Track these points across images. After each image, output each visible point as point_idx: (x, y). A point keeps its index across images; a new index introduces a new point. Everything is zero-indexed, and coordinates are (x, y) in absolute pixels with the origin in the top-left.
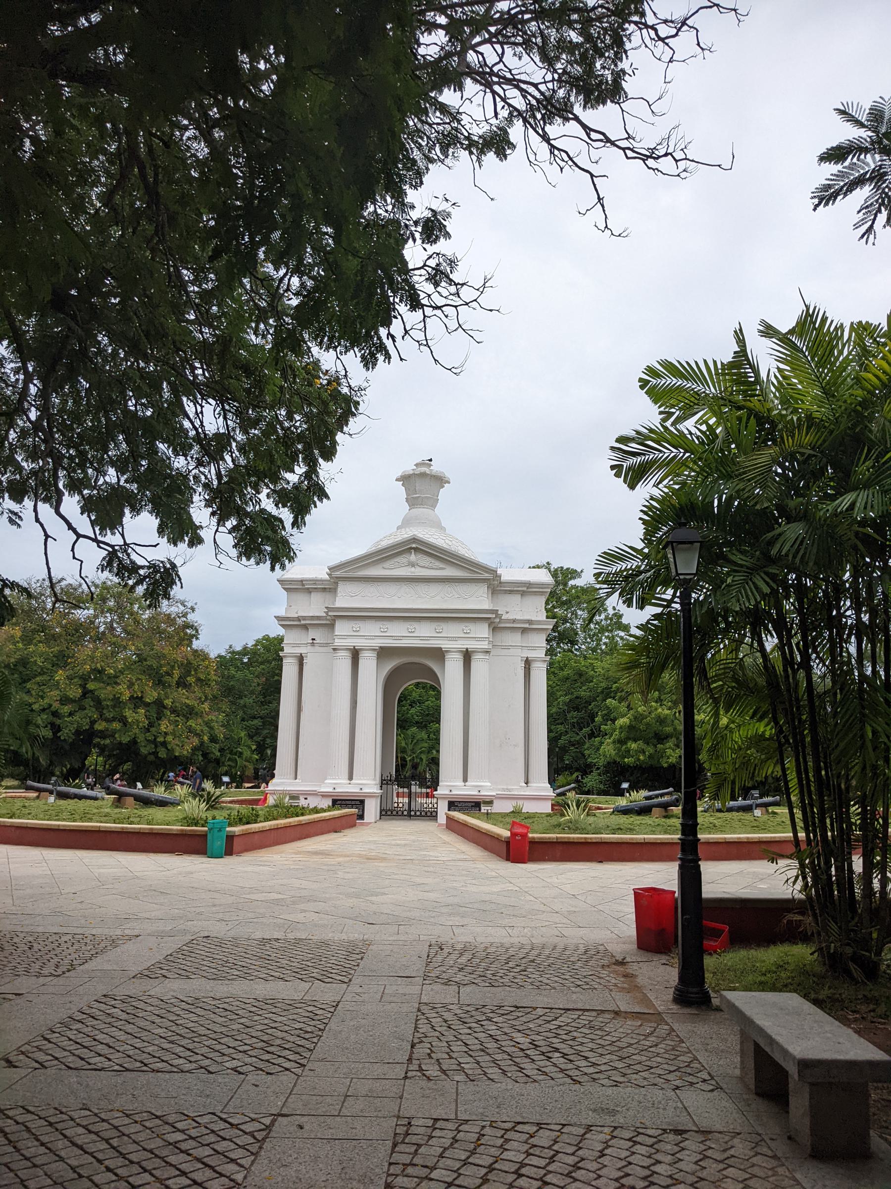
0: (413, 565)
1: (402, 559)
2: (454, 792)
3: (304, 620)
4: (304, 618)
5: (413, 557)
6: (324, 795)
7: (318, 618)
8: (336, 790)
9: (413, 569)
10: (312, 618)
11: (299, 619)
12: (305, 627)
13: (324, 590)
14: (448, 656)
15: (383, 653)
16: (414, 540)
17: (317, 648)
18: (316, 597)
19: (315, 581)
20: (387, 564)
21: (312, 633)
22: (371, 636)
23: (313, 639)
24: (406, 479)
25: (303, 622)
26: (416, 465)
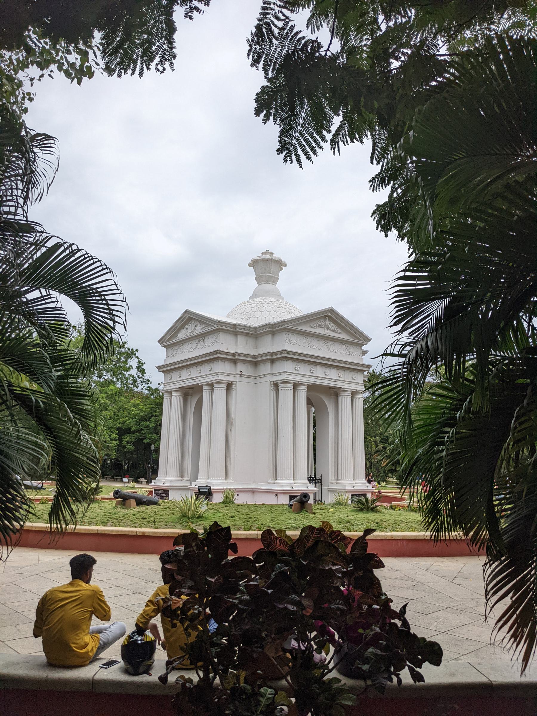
0: (328, 328)
1: (321, 323)
2: (356, 488)
4: (239, 354)
5: (328, 322)
6: (284, 493)
7: (248, 356)
8: (295, 489)
9: (326, 331)
11: (234, 355)
12: (235, 362)
13: (247, 335)
14: (342, 394)
15: (311, 388)
16: (331, 310)
17: (243, 379)
18: (241, 339)
19: (245, 327)
21: (240, 367)
22: (307, 375)
23: (241, 371)
24: (254, 263)
25: (237, 357)
26: (263, 253)
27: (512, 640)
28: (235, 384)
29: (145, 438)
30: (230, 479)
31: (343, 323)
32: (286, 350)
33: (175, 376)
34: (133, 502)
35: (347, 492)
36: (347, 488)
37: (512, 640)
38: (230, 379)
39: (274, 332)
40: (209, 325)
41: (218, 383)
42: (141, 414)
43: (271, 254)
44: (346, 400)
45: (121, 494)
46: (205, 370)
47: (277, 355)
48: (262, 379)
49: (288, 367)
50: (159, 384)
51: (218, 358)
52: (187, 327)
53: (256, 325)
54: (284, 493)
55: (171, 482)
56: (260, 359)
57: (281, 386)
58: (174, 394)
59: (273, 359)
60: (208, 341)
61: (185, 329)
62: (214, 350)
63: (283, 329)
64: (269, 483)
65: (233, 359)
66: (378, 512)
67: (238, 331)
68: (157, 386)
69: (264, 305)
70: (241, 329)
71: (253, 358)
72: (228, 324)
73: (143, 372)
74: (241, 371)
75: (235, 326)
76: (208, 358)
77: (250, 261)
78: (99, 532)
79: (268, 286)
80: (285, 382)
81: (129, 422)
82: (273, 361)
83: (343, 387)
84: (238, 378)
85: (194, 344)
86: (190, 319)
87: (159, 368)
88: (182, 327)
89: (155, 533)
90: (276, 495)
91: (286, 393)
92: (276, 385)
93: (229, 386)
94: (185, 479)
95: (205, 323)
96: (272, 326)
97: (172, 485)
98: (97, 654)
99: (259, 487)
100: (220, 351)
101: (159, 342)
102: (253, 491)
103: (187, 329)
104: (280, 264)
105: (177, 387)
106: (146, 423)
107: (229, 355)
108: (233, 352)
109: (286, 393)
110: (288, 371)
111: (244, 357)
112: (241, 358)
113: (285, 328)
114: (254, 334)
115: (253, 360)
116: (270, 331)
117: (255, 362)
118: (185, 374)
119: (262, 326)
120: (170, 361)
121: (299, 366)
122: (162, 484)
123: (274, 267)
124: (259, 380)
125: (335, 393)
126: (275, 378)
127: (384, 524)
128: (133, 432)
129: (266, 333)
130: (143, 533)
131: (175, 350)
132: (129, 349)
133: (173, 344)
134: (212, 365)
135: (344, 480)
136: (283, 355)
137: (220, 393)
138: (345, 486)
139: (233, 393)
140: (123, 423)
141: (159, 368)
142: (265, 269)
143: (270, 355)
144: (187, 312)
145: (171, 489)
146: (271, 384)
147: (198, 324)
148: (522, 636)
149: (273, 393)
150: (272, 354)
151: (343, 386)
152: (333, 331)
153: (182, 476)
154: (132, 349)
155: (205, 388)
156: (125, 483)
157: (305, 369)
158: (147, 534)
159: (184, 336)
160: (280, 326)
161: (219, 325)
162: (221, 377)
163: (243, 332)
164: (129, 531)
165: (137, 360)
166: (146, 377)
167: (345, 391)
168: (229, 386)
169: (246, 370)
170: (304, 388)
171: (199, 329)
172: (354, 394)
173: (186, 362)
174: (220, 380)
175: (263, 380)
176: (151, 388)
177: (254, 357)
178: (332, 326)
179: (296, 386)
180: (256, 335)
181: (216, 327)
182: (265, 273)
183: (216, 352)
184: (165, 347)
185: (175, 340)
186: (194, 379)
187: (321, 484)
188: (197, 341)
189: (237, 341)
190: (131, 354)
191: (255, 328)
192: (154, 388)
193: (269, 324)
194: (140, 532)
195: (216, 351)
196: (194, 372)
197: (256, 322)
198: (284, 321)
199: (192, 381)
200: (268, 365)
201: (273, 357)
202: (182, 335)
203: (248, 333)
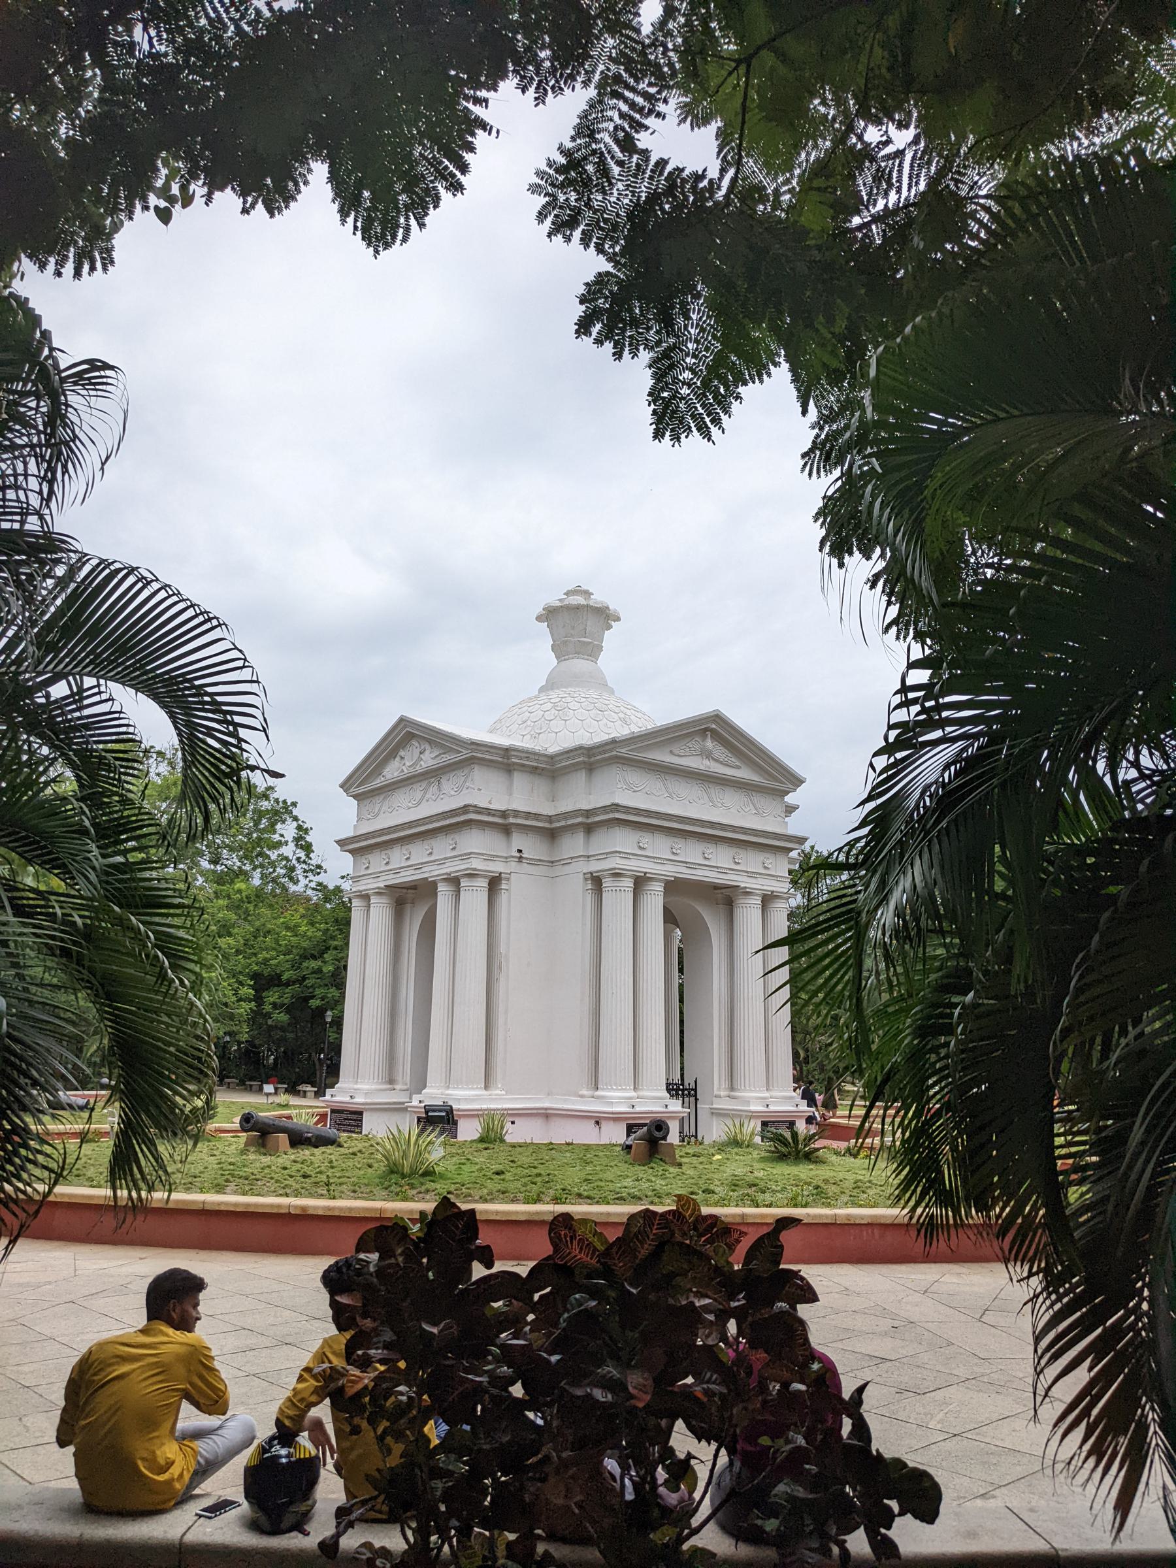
0: (709, 756)
1: (695, 744)
2: (772, 1108)
3: (515, 817)
4: (516, 814)
5: (709, 744)
6: (616, 1118)
7: (536, 816)
8: (637, 1109)
9: (706, 762)
10: (528, 815)
11: (504, 814)
13: (534, 771)
14: (741, 901)
15: (673, 887)
16: (717, 718)
17: (525, 867)
18: (520, 781)
19: (529, 754)
20: (676, 748)
21: (519, 841)
22: (665, 858)
23: (520, 851)
24: (550, 615)
25: (512, 820)
27: (1092, 1461)
28: (508, 879)
29: (312, 997)
30: (497, 1088)
31: (745, 746)
32: (617, 805)
33: (377, 862)
34: (283, 1138)
35: (752, 1116)
36: (753, 1108)
37: (1092, 1461)
38: (497, 867)
39: (591, 764)
40: (450, 750)
41: (471, 876)
42: (305, 944)
43: (587, 594)
44: (749, 915)
45: (257, 1123)
46: (441, 847)
47: (597, 815)
48: (566, 867)
49: (623, 840)
50: (343, 877)
51: (470, 821)
52: (402, 753)
53: (553, 749)
54: (615, 1120)
55: (368, 1093)
56: (563, 823)
57: (607, 883)
58: (373, 900)
59: (590, 823)
60: (449, 784)
61: (398, 759)
62: (462, 804)
63: (611, 758)
64: (582, 1096)
65: (504, 824)
66: (819, 1161)
67: (514, 764)
68: (339, 882)
69: (572, 705)
70: (521, 758)
71: (545, 821)
72: (492, 747)
73: (308, 848)
74: (520, 851)
75: (507, 751)
76: (448, 822)
77: (539, 610)
78: (208, 1207)
79: (579, 665)
80: (617, 875)
81: (280, 962)
82: (589, 829)
83: (742, 885)
84: (513, 866)
85: (417, 791)
86: (410, 736)
87: (341, 843)
88: (393, 754)
89: (329, 1208)
90: (597, 1123)
91: (618, 898)
92: (596, 882)
93: (494, 883)
94: (398, 1087)
95: (442, 746)
96: (589, 751)
97: (369, 1101)
98: (192, 1485)
99: (560, 1106)
100: (475, 806)
101: (342, 786)
102: (546, 1115)
103: (402, 758)
104: (605, 616)
105: (382, 885)
106: (314, 964)
107: (494, 815)
108: (503, 808)
109: (618, 898)
110: (623, 849)
111: (526, 818)
112: (519, 821)
113: (617, 757)
114: (549, 769)
115: (547, 825)
116: (584, 762)
117: (551, 831)
118: (397, 857)
119: (567, 752)
120: (366, 828)
121: (646, 839)
122: (347, 1099)
123: (591, 623)
124: (559, 870)
125: (726, 898)
126: (595, 866)
127: (832, 1190)
128: (287, 984)
129: (575, 767)
130: (304, 1208)
131: (376, 803)
132: (277, 801)
133: (372, 791)
134: (457, 837)
135: (745, 1091)
136: (611, 816)
137: (474, 897)
138: (748, 1103)
139: (503, 897)
140: (266, 962)
141: (341, 843)
142: (573, 628)
143: (582, 815)
144: (402, 720)
145: (366, 1110)
146: (586, 879)
147: (427, 746)
148: (1115, 1454)
149: (589, 898)
150: (588, 813)
151: (744, 882)
152: (721, 763)
153: (391, 1081)
154: (285, 802)
155: (442, 887)
156: (268, 1095)
157: (659, 846)
158: (311, 1212)
159: (396, 774)
160: (604, 752)
161: (473, 750)
162: (477, 864)
163: (523, 765)
164: (272, 1206)
165: (295, 824)
166: (315, 860)
167: (747, 893)
168: (494, 883)
169: (531, 846)
170: (659, 887)
171: (430, 759)
172: (767, 900)
173: (399, 831)
174: (475, 869)
175: (567, 869)
176: (326, 887)
177: (549, 819)
178: (719, 751)
179: (640, 882)
180: (553, 771)
181: (465, 754)
182: (572, 636)
183: (466, 809)
184: (354, 797)
185: (378, 782)
186: (419, 867)
187: (696, 1100)
188: (424, 784)
189: (511, 784)
190: (284, 811)
191: (552, 757)
192: (331, 887)
193: (580, 748)
194: (296, 1207)
195: (466, 806)
196: (418, 853)
197: (553, 742)
198: (614, 742)
199: (413, 872)
200: (580, 837)
201: (590, 820)
202: (393, 771)
203: (536, 768)
